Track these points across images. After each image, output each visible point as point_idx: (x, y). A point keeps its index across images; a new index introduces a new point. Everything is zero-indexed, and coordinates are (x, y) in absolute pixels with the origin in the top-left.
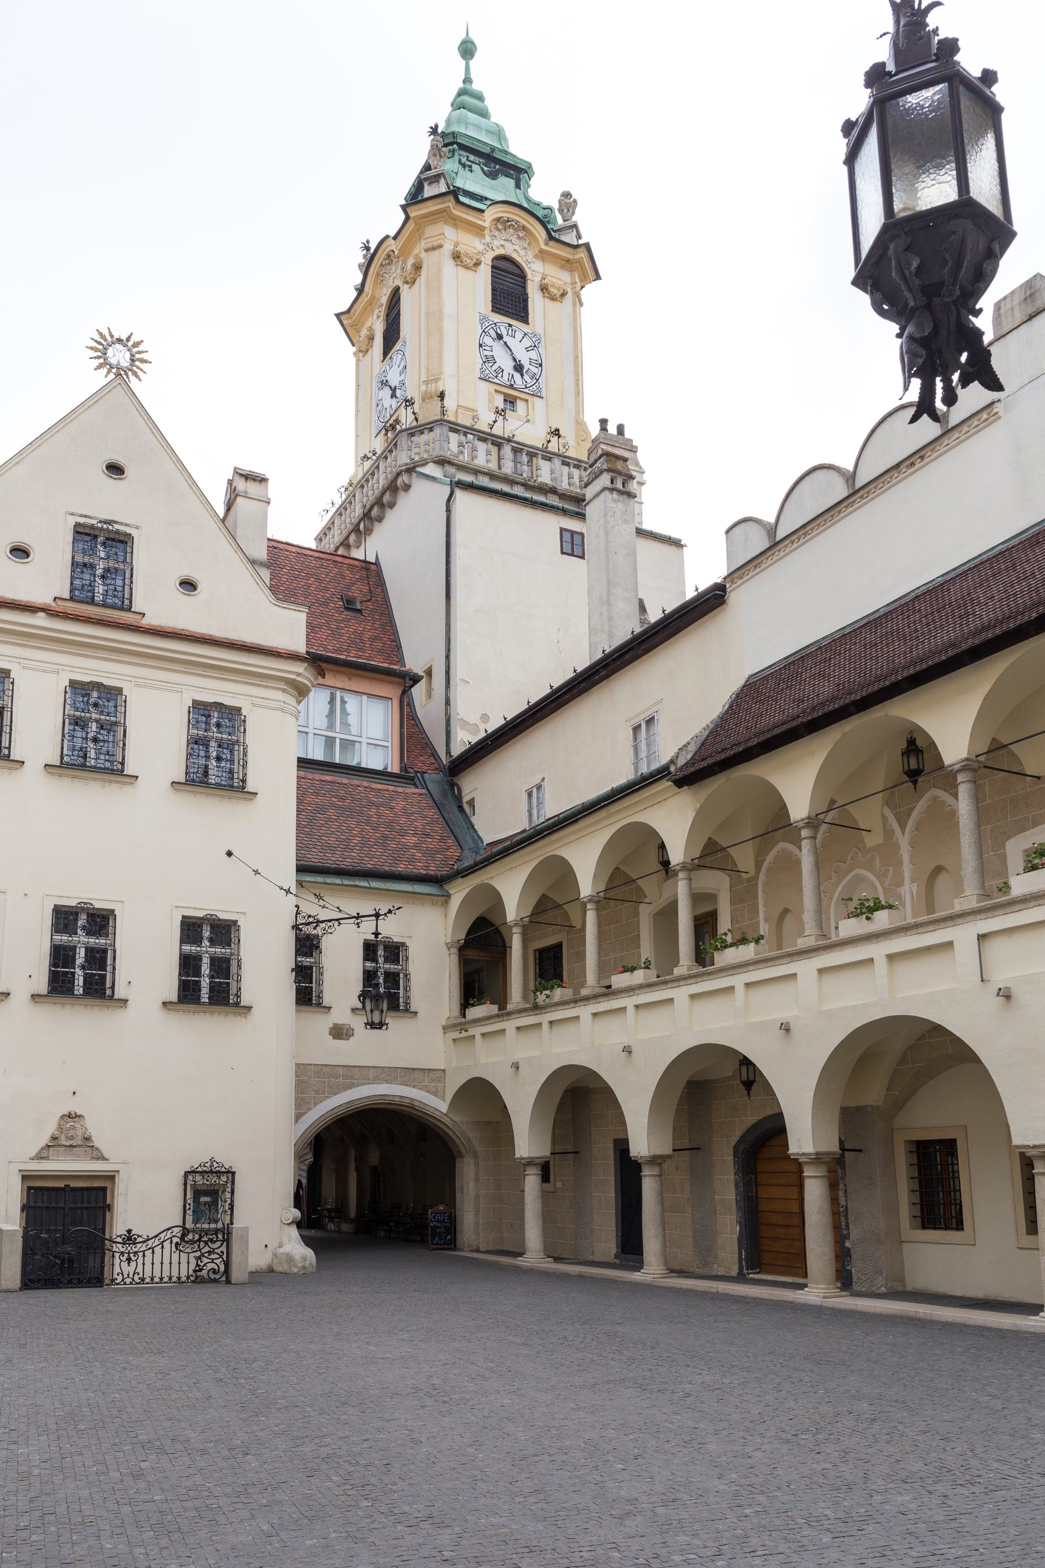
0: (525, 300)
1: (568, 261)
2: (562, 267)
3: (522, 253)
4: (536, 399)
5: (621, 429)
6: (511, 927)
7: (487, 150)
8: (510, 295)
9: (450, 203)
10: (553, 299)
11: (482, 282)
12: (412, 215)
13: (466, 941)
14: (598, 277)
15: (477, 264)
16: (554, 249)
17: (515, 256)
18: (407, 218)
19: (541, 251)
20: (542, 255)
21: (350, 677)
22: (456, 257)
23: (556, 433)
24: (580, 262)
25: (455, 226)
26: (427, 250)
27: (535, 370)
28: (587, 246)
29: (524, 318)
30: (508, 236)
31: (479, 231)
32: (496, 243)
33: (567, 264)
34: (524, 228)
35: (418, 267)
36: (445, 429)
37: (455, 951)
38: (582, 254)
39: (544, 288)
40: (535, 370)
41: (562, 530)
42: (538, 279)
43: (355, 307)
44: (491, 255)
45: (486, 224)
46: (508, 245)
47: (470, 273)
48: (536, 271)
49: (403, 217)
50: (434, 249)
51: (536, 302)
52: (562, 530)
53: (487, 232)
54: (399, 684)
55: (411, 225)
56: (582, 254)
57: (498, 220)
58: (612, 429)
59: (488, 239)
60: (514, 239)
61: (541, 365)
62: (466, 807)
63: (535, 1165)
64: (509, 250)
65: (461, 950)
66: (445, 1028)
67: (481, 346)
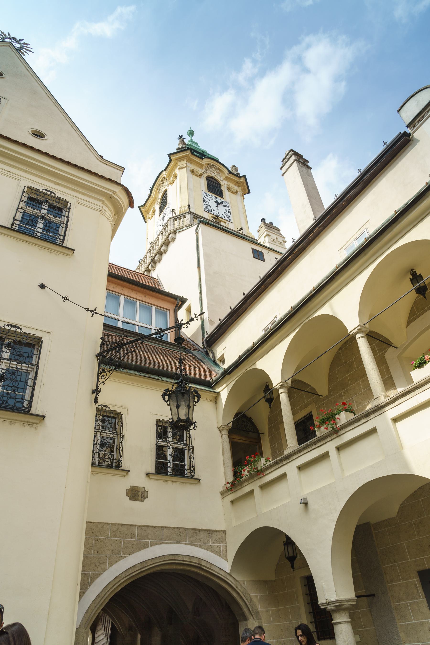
0: (221, 191)
1: (237, 182)
2: (235, 185)
3: (219, 177)
4: (230, 223)
5: (271, 223)
6: (277, 390)
7: (201, 152)
8: (214, 187)
9: (188, 153)
10: (233, 193)
11: (203, 184)
12: (172, 158)
13: (233, 423)
14: (249, 192)
15: (201, 175)
16: (231, 176)
17: (215, 177)
18: (171, 161)
19: (226, 177)
20: (227, 179)
21: (146, 295)
22: (192, 172)
23: (241, 229)
24: (241, 183)
25: (191, 163)
26: (179, 169)
27: (228, 213)
28: (245, 176)
29: (222, 196)
30: (213, 171)
31: (201, 166)
32: (208, 172)
33: (237, 184)
34: (219, 169)
35: (176, 176)
36: (192, 216)
37: (225, 432)
38: (242, 180)
39: (229, 189)
40: (228, 213)
41: (252, 249)
42: (226, 186)
43: (147, 203)
44: (205, 175)
45: (204, 164)
46: (212, 173)
47: (198, 178)
48: (224, 185)
49: (168, 160)
50: (182, 168)
51: (226, 193)
52: (252, 249)
53: (204, 167)
54: (173, 303)
55: (172, 163)
56: (242, 180)
57: (208, 164)
58: (267, 222)
59: (204, 170)
60: (215, 172)
61: (230, 212)
62: (218, 362)
63: (344, 609)
64: (213, 175)
65: (231, 432)
66: (223, 494)
67: (204, 201)
